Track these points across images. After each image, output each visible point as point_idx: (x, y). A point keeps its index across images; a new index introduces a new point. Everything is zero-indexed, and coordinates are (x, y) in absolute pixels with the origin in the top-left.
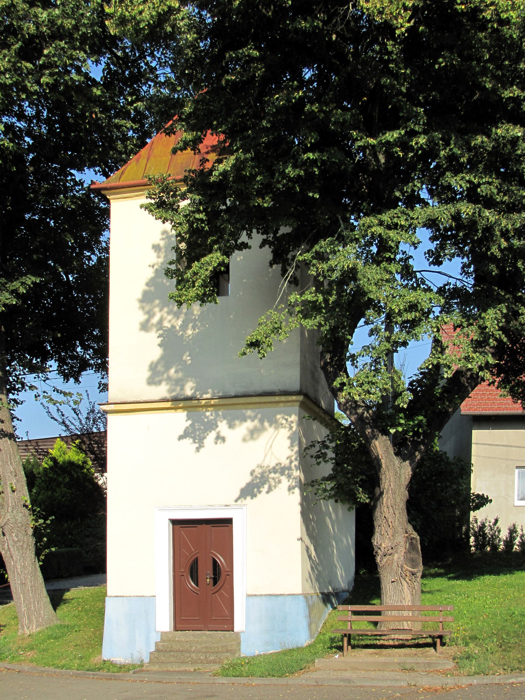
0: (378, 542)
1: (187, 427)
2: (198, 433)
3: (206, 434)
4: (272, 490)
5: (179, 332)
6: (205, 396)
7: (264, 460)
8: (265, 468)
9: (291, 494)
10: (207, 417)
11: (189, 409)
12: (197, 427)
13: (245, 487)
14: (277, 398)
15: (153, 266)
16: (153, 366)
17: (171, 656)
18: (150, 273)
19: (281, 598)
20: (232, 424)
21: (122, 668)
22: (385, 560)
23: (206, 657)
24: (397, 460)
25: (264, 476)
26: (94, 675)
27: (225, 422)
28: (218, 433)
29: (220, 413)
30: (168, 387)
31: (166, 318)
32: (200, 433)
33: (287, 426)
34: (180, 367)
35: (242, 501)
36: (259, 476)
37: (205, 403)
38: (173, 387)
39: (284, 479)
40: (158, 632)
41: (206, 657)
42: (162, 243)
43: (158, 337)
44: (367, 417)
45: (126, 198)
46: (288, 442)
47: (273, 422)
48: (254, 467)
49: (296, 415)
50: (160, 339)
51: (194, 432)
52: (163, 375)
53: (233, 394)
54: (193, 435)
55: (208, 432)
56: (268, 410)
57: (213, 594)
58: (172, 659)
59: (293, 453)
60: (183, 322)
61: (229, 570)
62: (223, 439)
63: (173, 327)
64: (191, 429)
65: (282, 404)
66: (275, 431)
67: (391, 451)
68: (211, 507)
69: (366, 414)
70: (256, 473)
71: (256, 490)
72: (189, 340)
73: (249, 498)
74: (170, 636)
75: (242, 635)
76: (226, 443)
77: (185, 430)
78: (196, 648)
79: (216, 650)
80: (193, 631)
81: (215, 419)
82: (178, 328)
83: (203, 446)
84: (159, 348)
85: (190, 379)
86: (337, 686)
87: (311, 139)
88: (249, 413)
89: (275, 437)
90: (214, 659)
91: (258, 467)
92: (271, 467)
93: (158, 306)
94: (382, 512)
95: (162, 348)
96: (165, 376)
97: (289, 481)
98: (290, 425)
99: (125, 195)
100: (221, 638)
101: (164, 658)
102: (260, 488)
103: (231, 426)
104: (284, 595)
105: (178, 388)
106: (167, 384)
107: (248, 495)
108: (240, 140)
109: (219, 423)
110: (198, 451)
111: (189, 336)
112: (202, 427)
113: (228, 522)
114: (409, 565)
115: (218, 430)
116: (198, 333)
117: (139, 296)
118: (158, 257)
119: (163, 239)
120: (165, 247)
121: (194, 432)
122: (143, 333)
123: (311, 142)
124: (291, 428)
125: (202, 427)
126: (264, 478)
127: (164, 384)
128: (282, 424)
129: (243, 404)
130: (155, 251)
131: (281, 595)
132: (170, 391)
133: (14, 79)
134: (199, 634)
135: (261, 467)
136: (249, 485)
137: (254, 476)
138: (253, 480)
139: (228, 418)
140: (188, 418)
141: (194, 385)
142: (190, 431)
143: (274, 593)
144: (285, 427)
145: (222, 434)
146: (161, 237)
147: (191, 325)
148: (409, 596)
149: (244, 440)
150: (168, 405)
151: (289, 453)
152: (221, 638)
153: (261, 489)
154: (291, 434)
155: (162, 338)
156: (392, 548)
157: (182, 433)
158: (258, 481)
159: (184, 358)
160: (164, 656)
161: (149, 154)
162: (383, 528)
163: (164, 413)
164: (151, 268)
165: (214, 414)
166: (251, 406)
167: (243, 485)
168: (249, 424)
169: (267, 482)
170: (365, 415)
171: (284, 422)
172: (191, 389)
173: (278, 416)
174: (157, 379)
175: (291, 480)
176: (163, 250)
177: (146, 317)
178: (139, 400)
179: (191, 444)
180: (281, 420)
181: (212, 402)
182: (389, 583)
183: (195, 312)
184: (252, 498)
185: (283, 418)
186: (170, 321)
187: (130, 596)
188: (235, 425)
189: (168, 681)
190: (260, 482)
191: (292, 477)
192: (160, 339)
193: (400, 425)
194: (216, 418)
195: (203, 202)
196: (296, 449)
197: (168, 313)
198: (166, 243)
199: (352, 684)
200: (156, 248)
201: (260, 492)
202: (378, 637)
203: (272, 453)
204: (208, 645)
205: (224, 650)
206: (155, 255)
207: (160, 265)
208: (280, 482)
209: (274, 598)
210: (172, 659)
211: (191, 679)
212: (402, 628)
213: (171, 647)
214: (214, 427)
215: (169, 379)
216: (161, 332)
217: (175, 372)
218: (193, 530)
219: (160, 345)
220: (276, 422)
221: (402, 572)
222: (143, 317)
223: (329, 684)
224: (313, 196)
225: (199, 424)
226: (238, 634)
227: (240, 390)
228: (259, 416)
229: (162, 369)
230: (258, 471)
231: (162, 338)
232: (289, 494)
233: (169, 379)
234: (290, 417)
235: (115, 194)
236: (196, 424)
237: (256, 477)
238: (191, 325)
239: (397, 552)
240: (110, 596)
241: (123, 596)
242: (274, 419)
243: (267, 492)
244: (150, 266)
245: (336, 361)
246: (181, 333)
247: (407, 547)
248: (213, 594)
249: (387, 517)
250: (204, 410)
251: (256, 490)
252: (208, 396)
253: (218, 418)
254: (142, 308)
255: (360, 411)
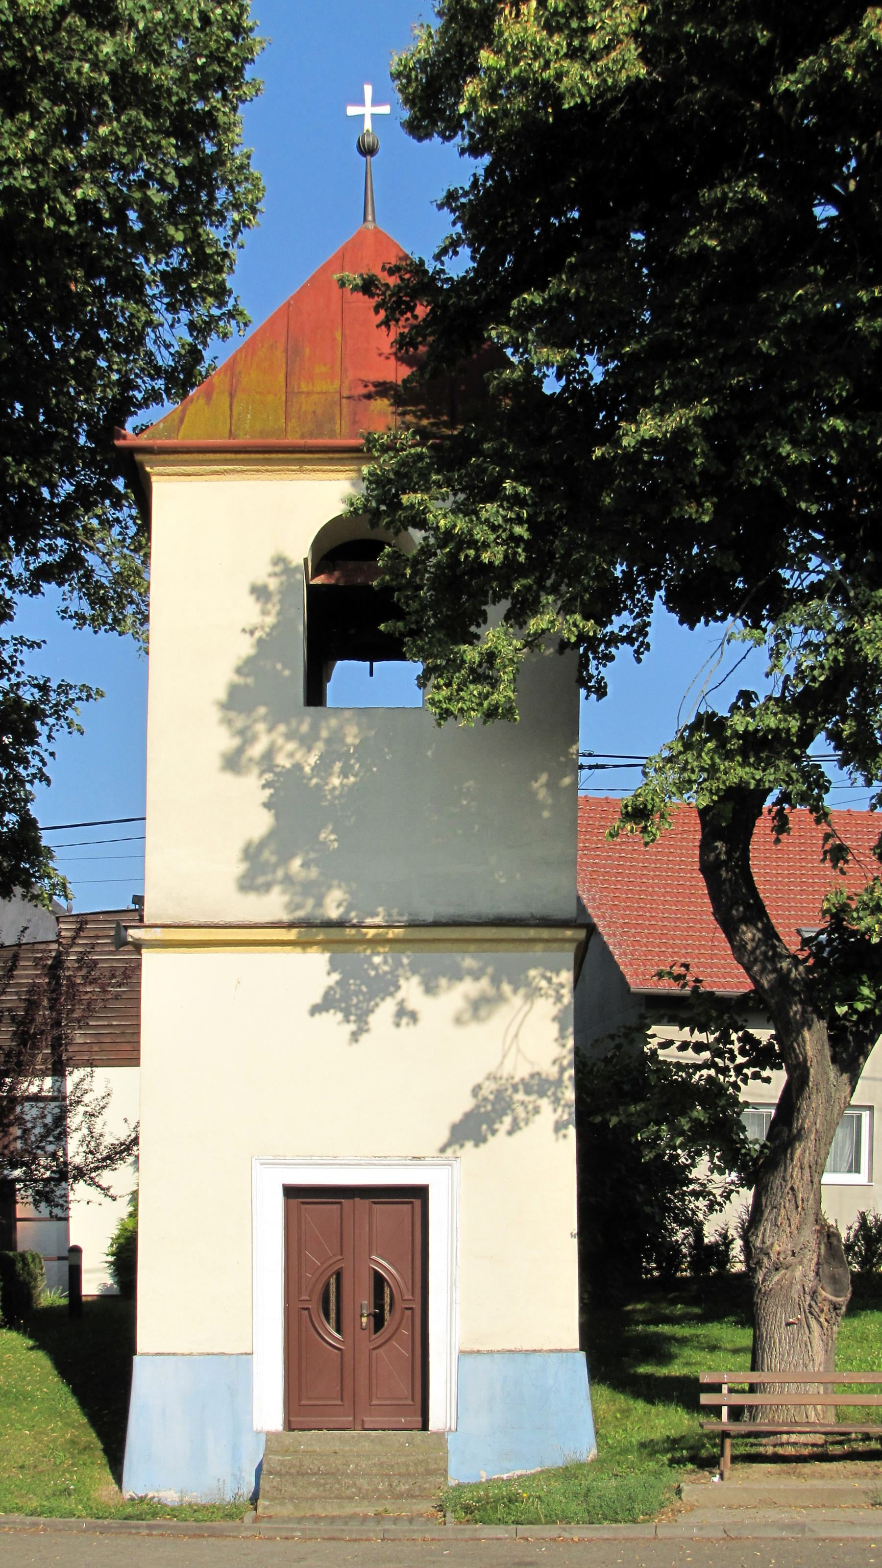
0: (766, 1240)
1: (331, 988)
2: (355, 1001)
3: (372, 1003)
4: (520, 1128)
5: (311, 779)
6: (369, 921)
7: (502, 1063)
8: (503, 1081)
9: (561, 1140)
10: (376, 967)
11: (334, 946)
12: (352, 987)
13: (462, 1121)
14: (532, 933)
15: (252, 633)
16: (252, 850)
17: (310, 1484)
18: (245, 647)
19: (533, 1358)
20: (432, 984)
21: (175, 1512)
22: (776, 1278)
23: (391, 1485)
24: (832, 1071)
25: (503, 1099)
26: (149, 1527)
27: (415, 980)
28: (401, 1003)
29: (405, 961)
30: (286, 898)
31: (281, 748)
32: (359, 1001)
33: (551, 992)
34: (312, 855)
35: (455, 1152)
36: (491, 1097)
37: (376, 935)
38: (298, 899)
39: (545, 1104)
40: (258, 1433)
41: (391, 1485)
42: (273, 584)
43: (264, 787)
44: (796, 980)
45: (189, 475)
46: (555, 1028)
47: (519, 982)
48: (479, 1078)
49: (569, 970)
50: (268, 792)
51: (346, 998)
52: (274, 871)
53: (430, 919)
54: (343, 1005)
55: (378, 1000)
56: (511, 956)
57: (374, 1349)
58: (313, 1491)
59: (565, 1052)
60: (321, 758)
61: (410, 1297)
62: (413, 1017)
63: (298, 767)
64: (338, 990)
65: (540, 946)
66: (525, 1002)
67: (828, 1053)
68: (381, 1160)
69: (794, 974)
70: (485, 1092)
71: (484, 1127)
72: (335, 798)
73: (469, 1145)
74: (287, 1442)
75: (450, 1437)
76: (420, 1024)
77: (326, 995)
78: (357, 1465)
79: (403, 1470)
80: (328, 1429)
81: (391, 972)
82: (307, 769)
83: (367, 1030)
84: (265, 811)
85: (335, 883)
86: (775, 1539)
87: (841, 390)
88: (469, 962)
89: (525, 1017)
90: (409, 1490)
91: (488, 1078)
92: (517, 1079)
93: (264, 719)
94: (788, 1178)
95: (273, 811)
96: (280, 873)
97: (555, 1110)
98: (557, 992)
99: (175, 469)
100: (402, 1445)
101: (294, 1489)
102: (494, 1123)
103: (430, 989)
104: (540, 1351)
105: (310, 903)
106: (284, 892)
107: (468, 1139)
108: (669, 378)
109: (402, 982)
110: (356, 1041)
111: (334, 788)
112: (364, 989)
113: (420, 1193)
114: (829, 1289)
115: (400, 995)
116: (355, 784)
117: (222, 694)
118: (264, 613)
119: (275, 574)
120: (280, 592)
121: (346, 998)
122: (228, 777)
123: (840, 396)
124: (559, 998)
125: (364, 989)
126: (503, 1104)
127: (276, 890)
128: (540, 989)
129: (513, 941)
130: (258, 599)
131: (535, 1351)
132: (291, 907)
133: (42, 183)
134: (353, 1437)
135: (495, 1078)
136: (468, 1116)
137: (480, 1097)
138: (478, 1107)
139: (423, 971)
140: (334, 967)
141: (347, 896)
142: (338, 996)
143: (519, 1347)
144: (547, 996)
145: (410, 1006)
146: (270, 569)
147: (338, 766)
148: (822, 1353)
149: (458, 1021)
150: (292, 934)
151: (555, 1051)
152: (402, 1445)
153: (496, 1126)
154: (560, 1011)
155: (272, 791)
156: (793, 1254)
157: (317, 999)
158: (489, 1107)
159: (323, 836)
160: (294, 1484)
161: (232, 385)
162: (783, 1212)
163: (276, 952)
164: (248, 636)
165: (390, 961)
166: (472, 947)
167: (457, 1116)
168: (469, 988)
169: (509, 1112)
170: (793, 975)
171: (544, 984)
172: (339, 906)
173: (532, 973)
174: (261, 880)
175: (560, 1110)
176: (276, 599)
177: (236, 742)
178: (216, 920)
179: (339, 1023)
180: (537, 980)
181: (391, 934)
182: (779, 1327)
183: (349, 740)
184: (476, 1145)
185: (544, 977)
186: (291, 755)
187: (190, 1354)
188: (437, 986)
189: (354, 1536)
190: (494, 1110)
191: (562, 1102)
192: (268, 792)
193: (863, 999)
194: (396, 969)
195: (530, 502)
196: (570, 1043)
197: (289, 737)
198: (282, 583)
199: (808, 1534)
200: (260, 592)
201: (494, 1132)
202: (752, 1440)
203: (519, 1050)
204: (383, 1459)
205: (421, 1469)
206: (256, 608)
207: (267, 630)
208: (537, 1110)
209: (519, 1358)
210: (313, 1491)
211: (414, 1531)
212: (804, 1420)
213: (301, 1465)
214: (392, 989)
215: (288, 880)
216: (269, 776)
217: (302, 865)
218: (330, 1210)
219: (267, 805)
220: (528, 984)
221: (813, 1303)
222: (226, 742)
223: (755, 1535)
224: (807, 508)
225: (358, 982)
226: (440, 1436)
227: (446, 910)
228: (490, 970)
229: (273, 859)
230: (489, 1087)
231: (272, 791)
232: (557, 1139)
233: (288, 880)
234: (558, 974)
235: (165, 463)
236: (351, 981)
237: (485, 1099)
238: (338, 766)
239: (801, 1263)
240: (143, 1354)
241: (174, 1354)
242: (522, 977)
243: (510, 1133)
244: (244, 630)
245: (738, 859)
246: (314, 781)
247: (823, 1252)
248: (374, 1349)
249: (796, 1187)
250: (368, 952)
251: (484, 1127)
252: (377, 920)
253: (400, 971)
254: (229, 722)
255: (785, 965)
